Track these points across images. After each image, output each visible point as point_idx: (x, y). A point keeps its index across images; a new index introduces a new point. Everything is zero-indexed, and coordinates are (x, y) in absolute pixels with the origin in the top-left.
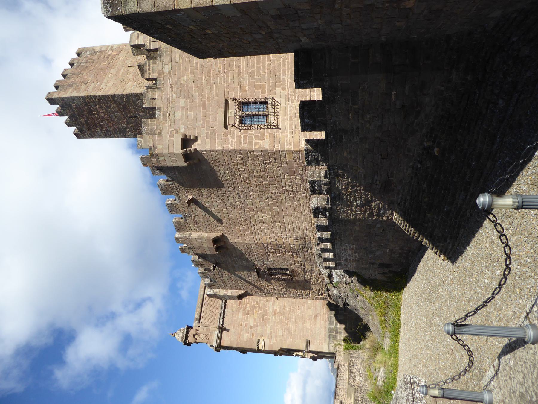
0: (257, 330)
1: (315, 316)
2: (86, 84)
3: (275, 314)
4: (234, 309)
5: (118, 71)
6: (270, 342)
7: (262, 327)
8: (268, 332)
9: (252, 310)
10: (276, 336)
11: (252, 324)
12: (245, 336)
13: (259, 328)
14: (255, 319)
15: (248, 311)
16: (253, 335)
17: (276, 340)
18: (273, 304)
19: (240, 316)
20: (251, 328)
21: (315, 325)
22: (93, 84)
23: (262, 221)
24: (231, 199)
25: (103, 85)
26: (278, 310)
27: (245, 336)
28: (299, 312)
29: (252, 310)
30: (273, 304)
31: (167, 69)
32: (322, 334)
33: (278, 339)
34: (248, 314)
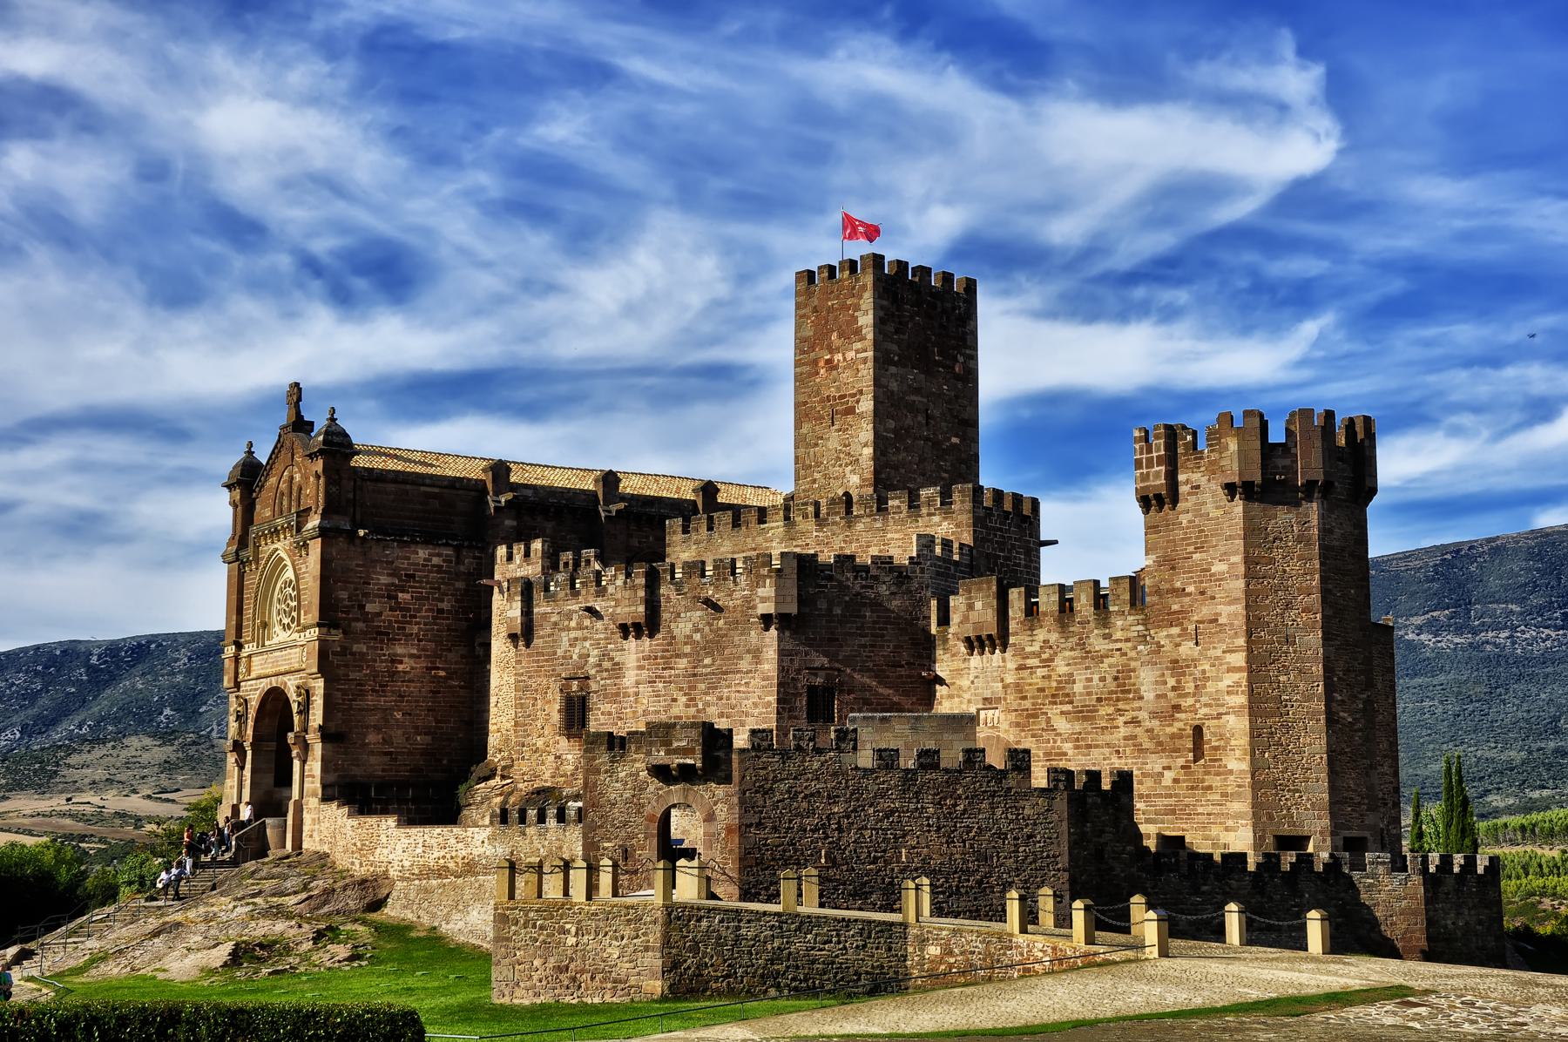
0: (357, 620)
1: (390, 753)
2: (897, 332)
3: (393, 661)
4: (397, 564)
5: (917, 391)
6: (335, 654)
7: (365, 633)
8: (355, 648)
9: (398, 607)
10: (346, 666)
11: (369, 608)
12: (344, 595)
13: (360, 625)
14: (380, 614)
15: (396, 598)
16: (347, 613)
17: (338, 666)
18: (412, 656)
19: (384, 580)
20: (362, 607)
21: (372, 753)
22: (895, 348)
24: (707, 661)
25: (893, 369)
26: (401, 668)
27: (344, 595)
28: (398, 715)
29: (398, 607)
30: (412, 656)
31: (883, 589)
32: (356, 771)
33: (341, 672)
34: (389, 597)
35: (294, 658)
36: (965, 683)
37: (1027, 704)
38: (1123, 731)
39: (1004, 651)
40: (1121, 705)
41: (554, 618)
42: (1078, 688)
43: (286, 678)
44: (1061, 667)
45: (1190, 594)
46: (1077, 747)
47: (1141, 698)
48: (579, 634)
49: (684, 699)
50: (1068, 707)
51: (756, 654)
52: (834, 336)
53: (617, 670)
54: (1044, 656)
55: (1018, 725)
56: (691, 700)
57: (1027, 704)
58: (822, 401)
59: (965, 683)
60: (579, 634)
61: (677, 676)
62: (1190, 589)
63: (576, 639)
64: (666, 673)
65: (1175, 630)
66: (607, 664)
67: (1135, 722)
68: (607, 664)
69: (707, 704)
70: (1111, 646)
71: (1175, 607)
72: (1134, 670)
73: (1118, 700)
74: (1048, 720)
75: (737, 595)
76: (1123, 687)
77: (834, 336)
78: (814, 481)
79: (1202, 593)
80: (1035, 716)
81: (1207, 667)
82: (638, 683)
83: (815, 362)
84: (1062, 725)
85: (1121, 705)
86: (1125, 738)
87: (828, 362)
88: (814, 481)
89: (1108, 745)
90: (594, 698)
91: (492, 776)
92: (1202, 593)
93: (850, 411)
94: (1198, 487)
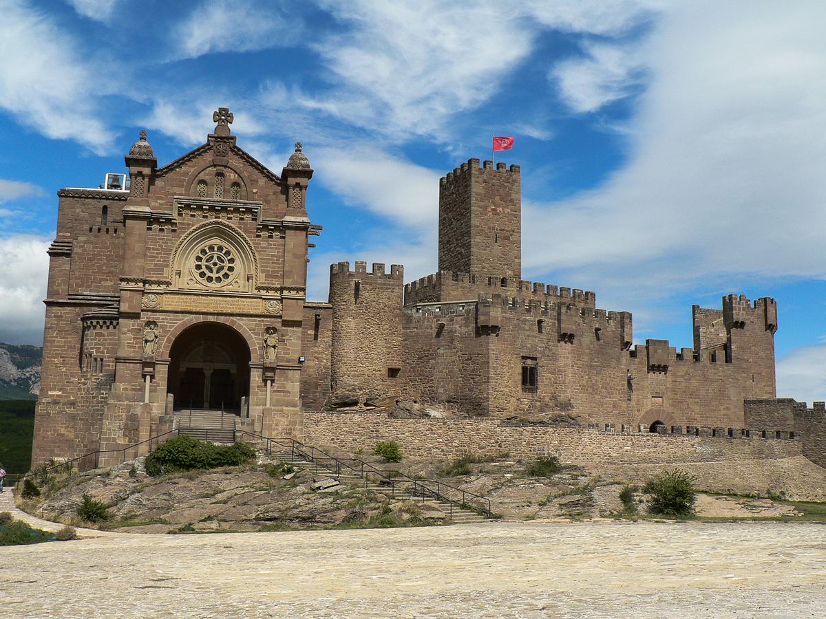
23: (582, 377)
35: (258, 307)
36: (646, 384)
37: (678, 397)
38: (723, 412)
39: (665, 374)
40: (721, 402)
41: (516, 321)
42: (702, 393)
43: (235, 319)
44: (694, 383)
45: (750, 362)
46: (701, 417)
47: (730, 400)
48: (529, 333)
49: (587, 377)
50: (696, 400)
51: (619, 360)
52: (497, 198)
53: (554, 357)
54: (686, 377)
55: (673, 405)
56: (590, 378)
57: (678, 397)
58: (489, 228)
59: (646, 384)
60: (529, 333)
61: (583, 364)
62: (751, 360)
63: (529, 336)
64: (579, 362)
65: (744, 375)
66: (547, 352)
67: (728, 409)
68: (547, 352)
69: (596, 381)
70: (717, 378)
71: (745, 366)
72: (727, 388)
73: (720, 399)
74: (688, 405)
75: (608, 329)
76: (722, 394)
77: (497, 198)
78: (484, 268)
79: (756, 363)
80: (682, 402)
81: (758, 391)
82: (566, 365)
83: (486, 207)
84: (697, 409)
85: (721, 402)
86: (723, 415)
87: (492, 209)
88: (484, 268)
89: (716, 417)
90: (540, 370)
91: (355, 403)
92: (756, 363)
93: (507, 238)
94: (753, 322)
